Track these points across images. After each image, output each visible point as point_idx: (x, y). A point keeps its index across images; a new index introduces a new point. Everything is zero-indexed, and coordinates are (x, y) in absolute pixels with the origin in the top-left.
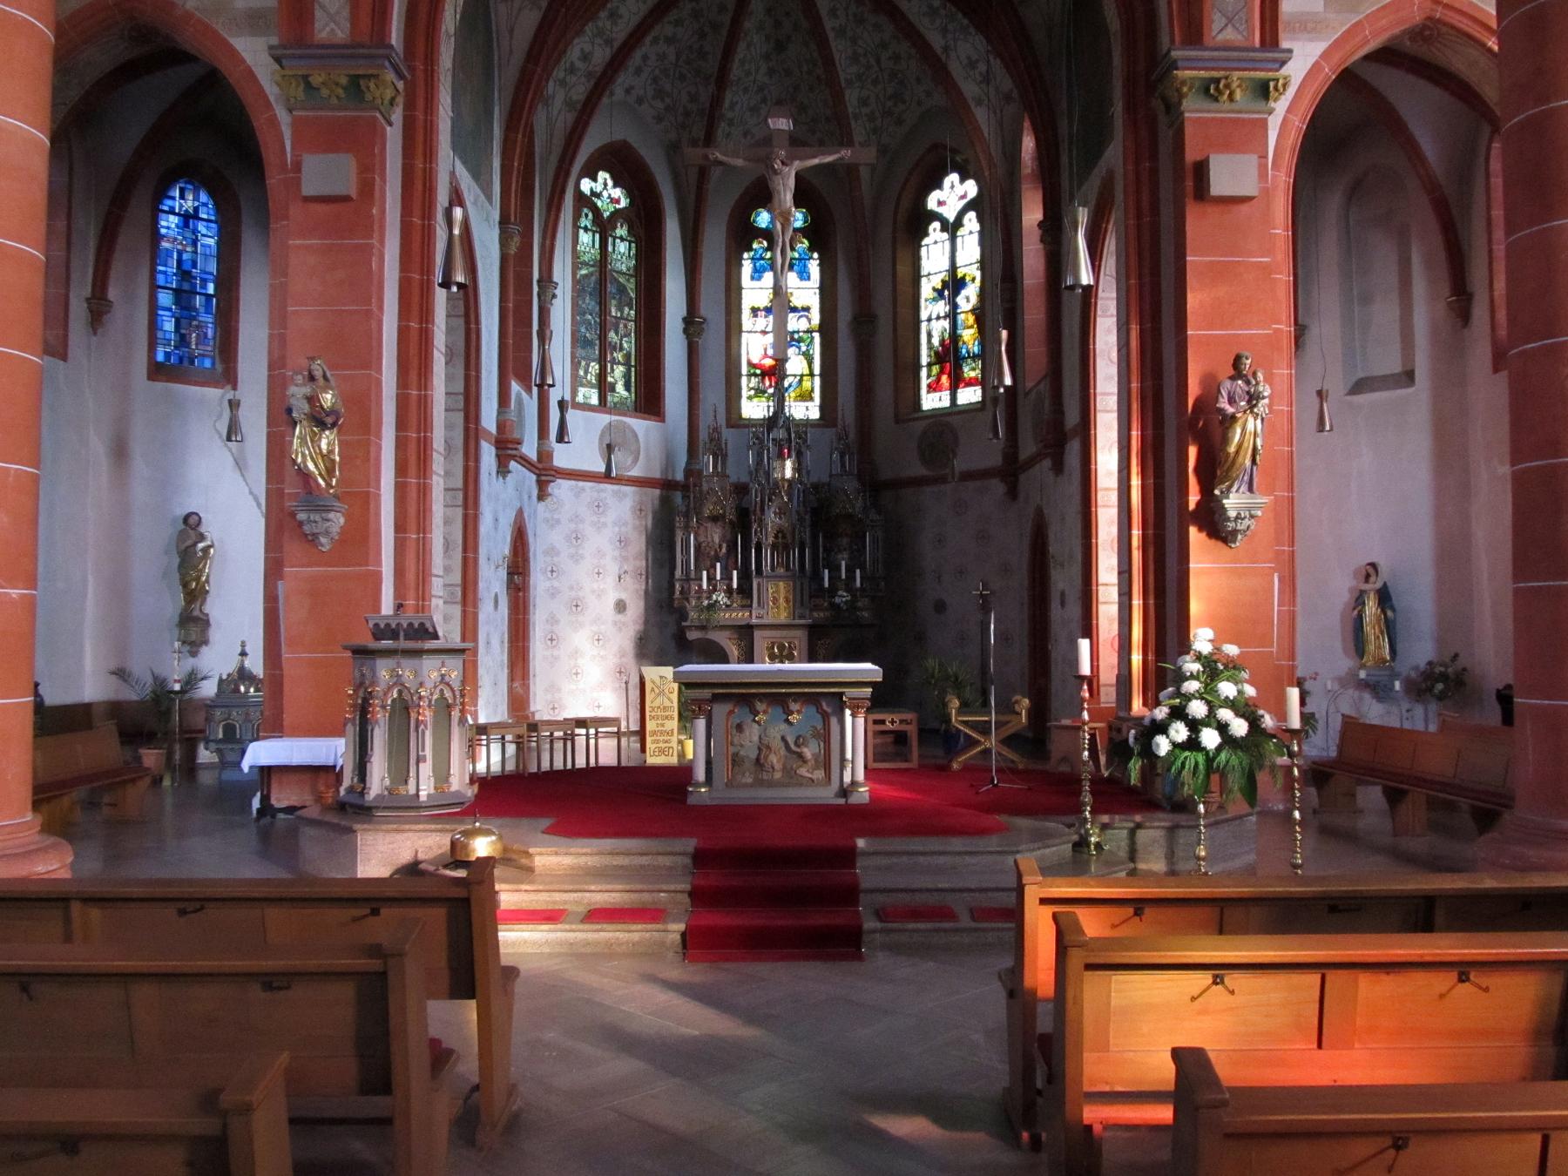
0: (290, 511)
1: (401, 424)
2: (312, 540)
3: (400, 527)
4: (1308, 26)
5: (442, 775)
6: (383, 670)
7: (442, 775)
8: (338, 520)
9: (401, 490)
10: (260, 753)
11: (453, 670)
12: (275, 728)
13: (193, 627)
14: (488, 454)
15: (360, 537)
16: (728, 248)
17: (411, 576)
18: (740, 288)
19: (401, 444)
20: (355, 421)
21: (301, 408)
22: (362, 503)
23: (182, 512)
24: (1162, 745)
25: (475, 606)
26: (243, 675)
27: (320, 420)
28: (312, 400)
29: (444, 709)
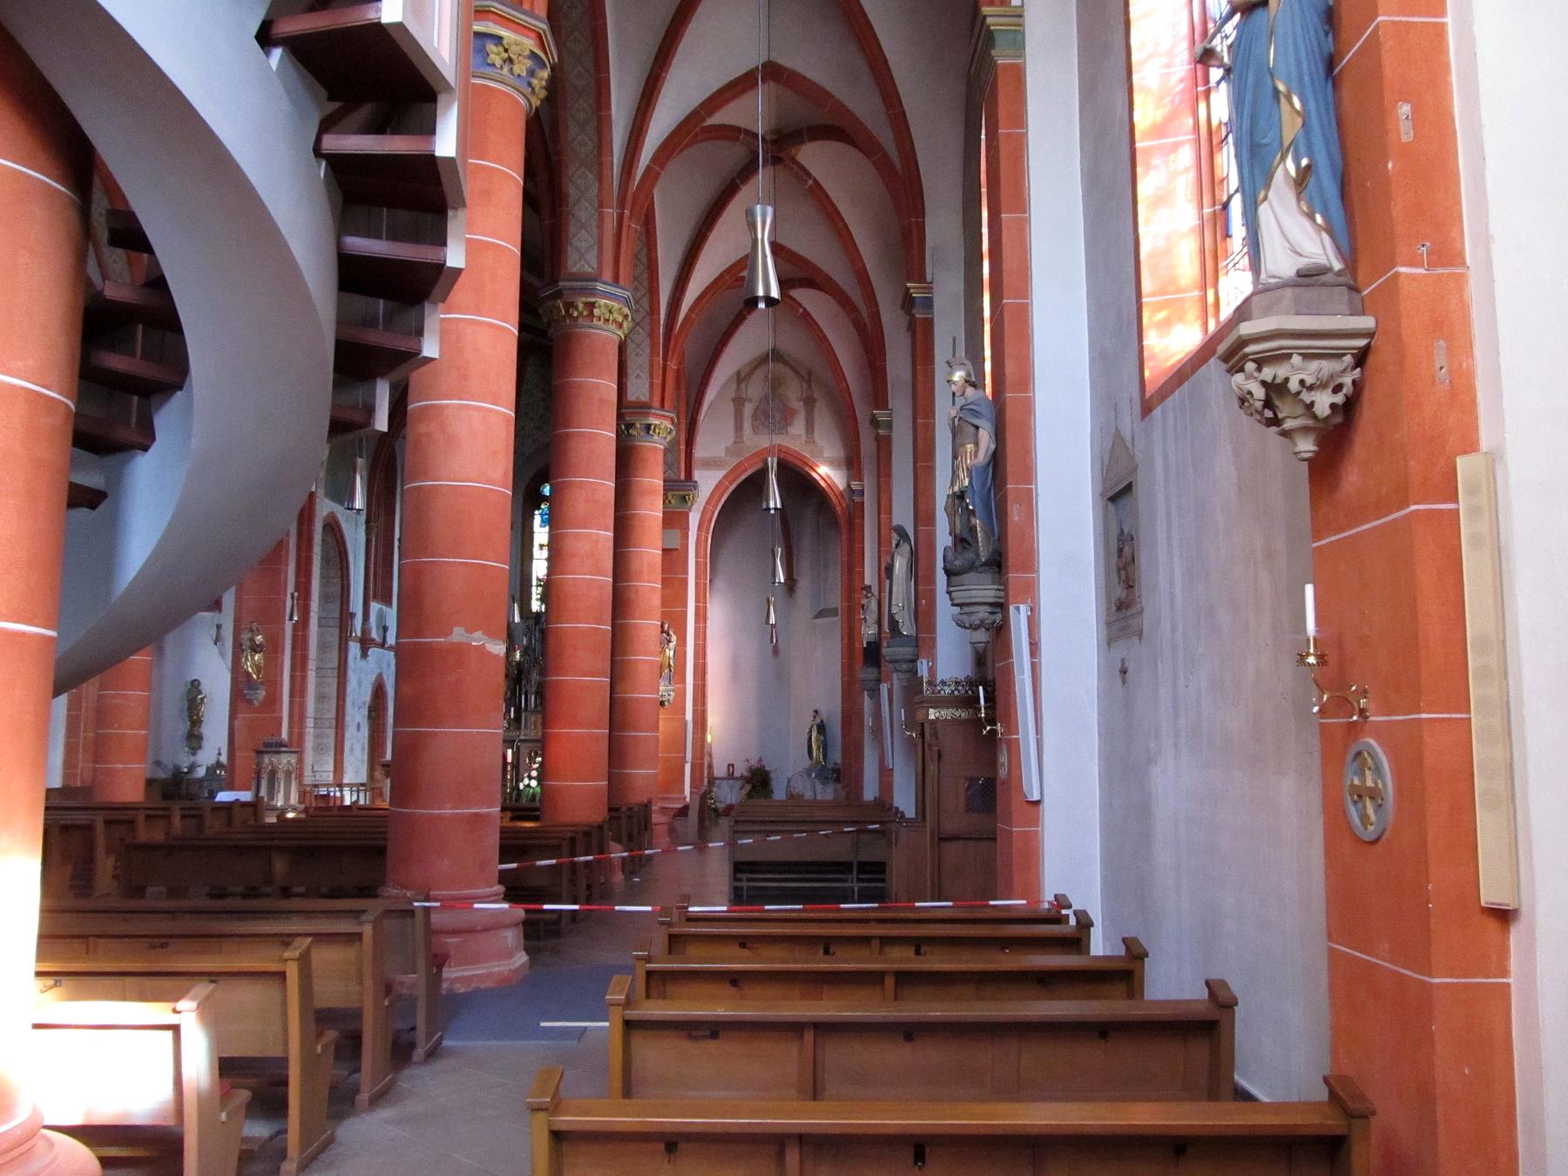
0: (241, 687)
1: (294, 648)
2: (250, 702)
3: (292, 695)
4: (710, 464)
5: (287, 798)
6: (266, 759)
7: (287, 798)
8: (262, 694)
9: (292, 678)
10: (224, 796)
11: (293, 759)
12: (231, 787)
13: (194, 740)
14: (354, 649)
15: (272, 701)
16: (525, 502)
17: (296, 718)
18: (532, 533)
19: (293, 658)
20: (272, 649)
21: (246, 644)
22: (273, 684)
23: (190, 679)
24: (521, 786)
25: (343, 730)
26: (219, 764)
27: (255, 649)
28: (252, 640)
29: (288, 774)
